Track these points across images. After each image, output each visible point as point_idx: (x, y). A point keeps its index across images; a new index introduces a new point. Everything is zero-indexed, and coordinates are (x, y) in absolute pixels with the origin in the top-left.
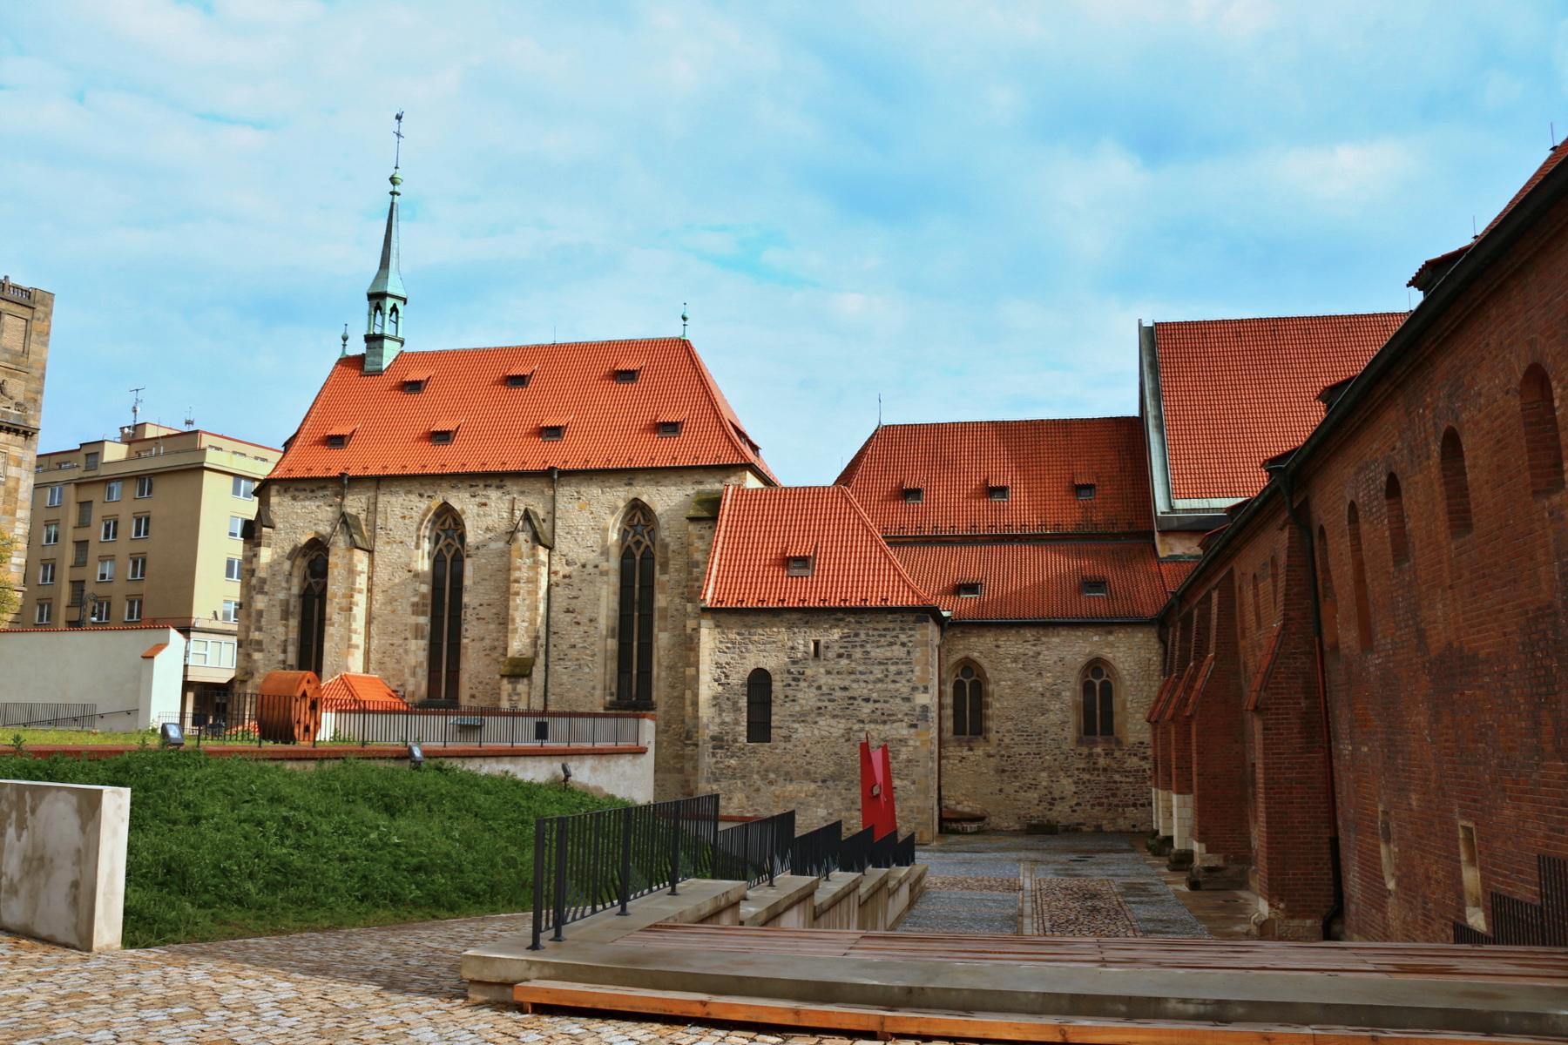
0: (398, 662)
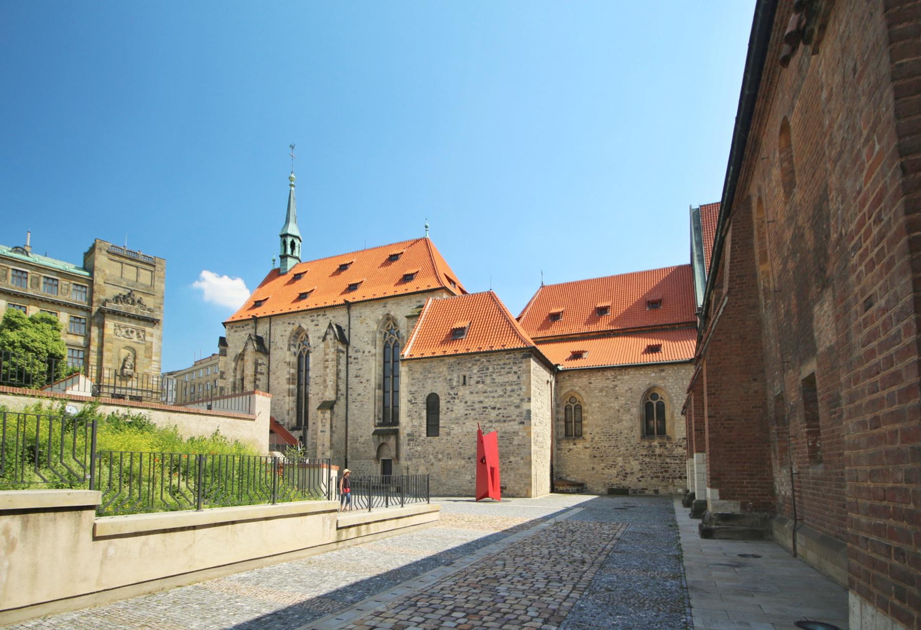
0: (281, 408)
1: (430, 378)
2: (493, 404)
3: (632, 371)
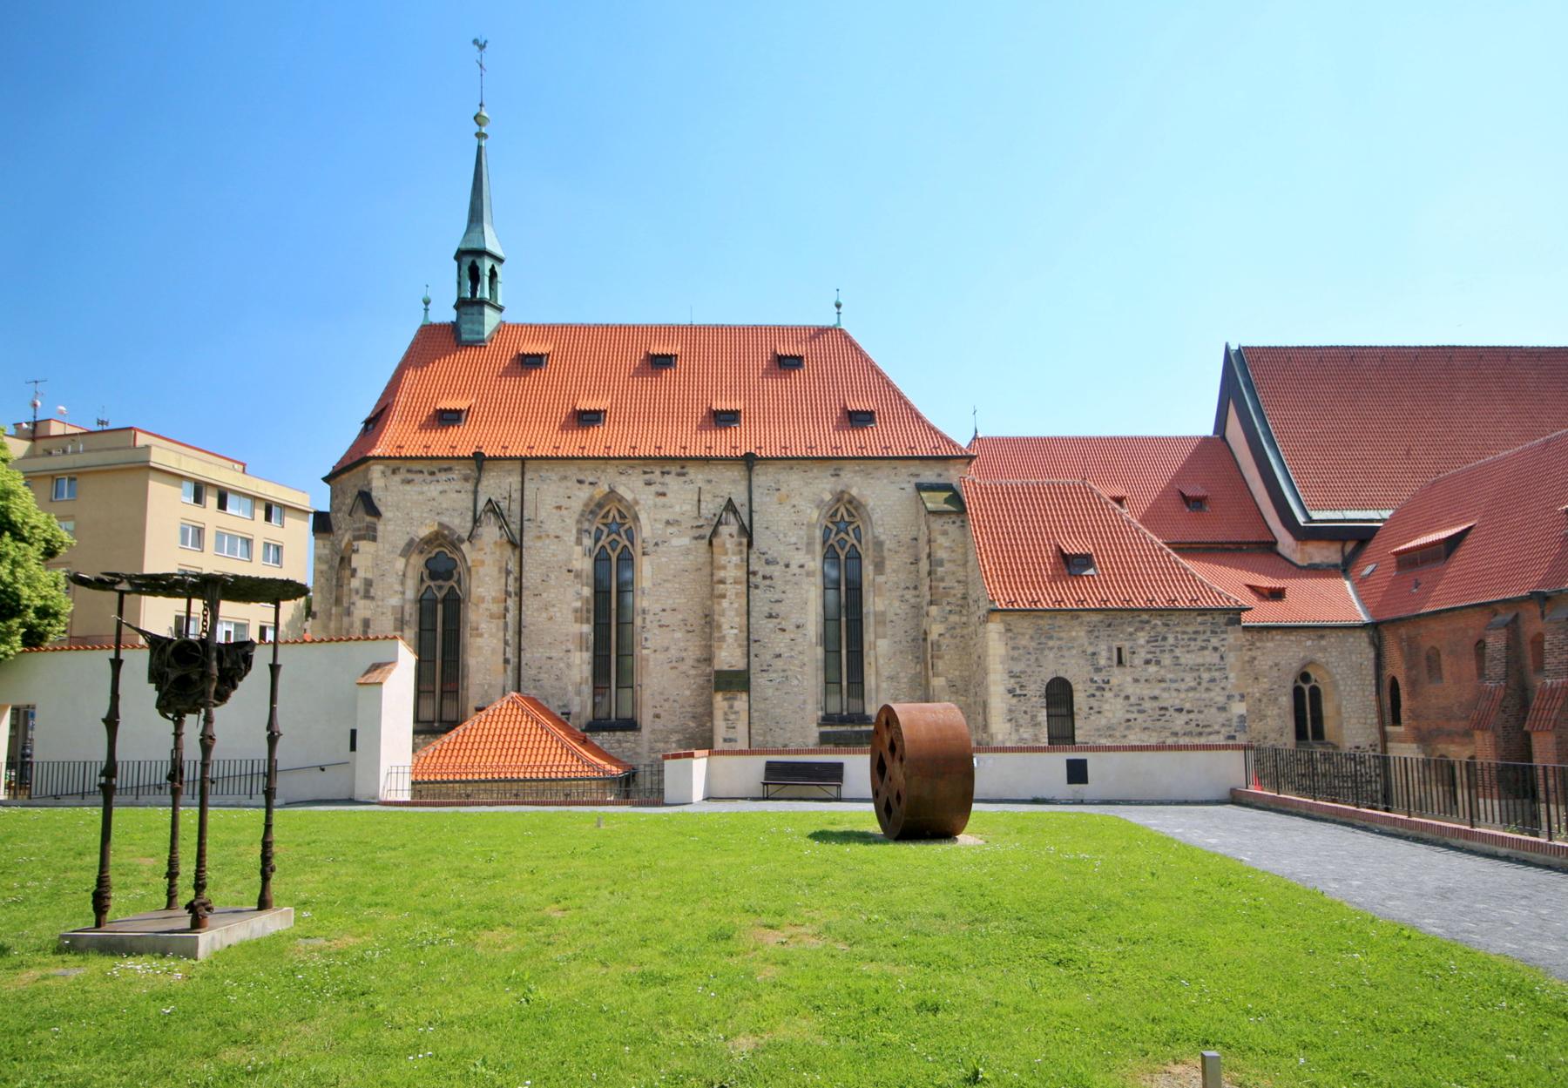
0: (558, 678)
1: (1051, 649)
3: (1278, 636)
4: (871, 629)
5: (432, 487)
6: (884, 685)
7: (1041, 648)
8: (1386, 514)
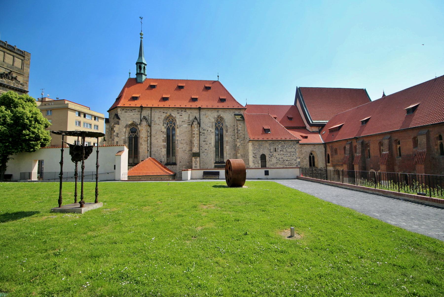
1: (262, 148)
2: (287, 159)
3: (306, 146)
4: (225, 144)
5: (131, 113)
6: (228, 156)
7: (260, 148)
8: (327, 121)
